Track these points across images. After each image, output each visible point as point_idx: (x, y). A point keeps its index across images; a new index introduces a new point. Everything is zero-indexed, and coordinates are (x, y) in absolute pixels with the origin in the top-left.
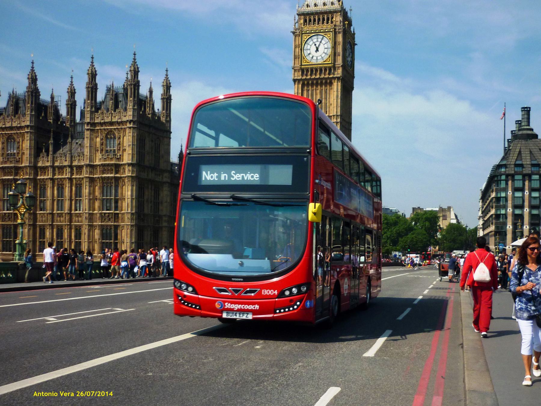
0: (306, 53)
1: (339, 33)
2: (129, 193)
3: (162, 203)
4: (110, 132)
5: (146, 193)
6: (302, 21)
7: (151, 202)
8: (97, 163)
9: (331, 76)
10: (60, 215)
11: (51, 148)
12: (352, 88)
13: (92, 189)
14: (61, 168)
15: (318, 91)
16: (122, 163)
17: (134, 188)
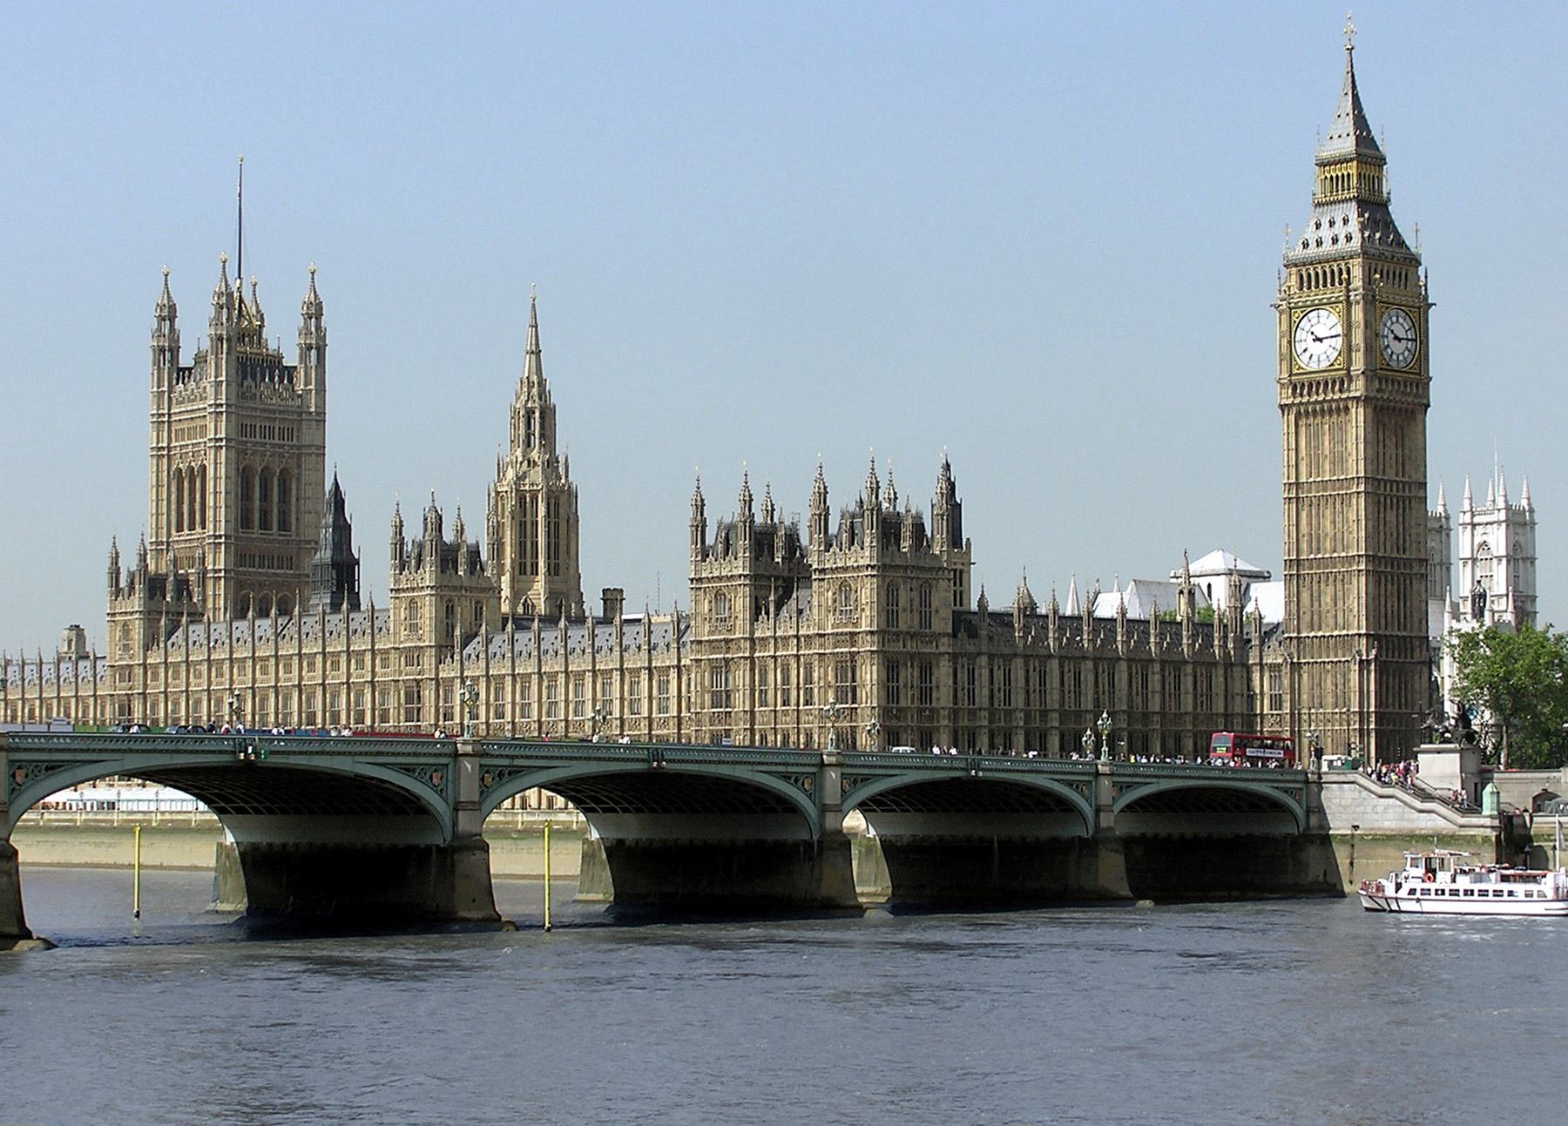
0: (1300, 347)
1: (1357, 302)
2: (868, 677)
3: (938, 687)
4: (844, 582)
5: (902, 674)
6: (1294, 280)
7: (912, 687)
8: (830, 631)
9: (1344, 396)
10: (785, 713)
11: (772, 610)
12: (1428, 406)
13: (822, 670)
14: (785, 639)
15: (1327, 426)
16: (858, 630)
17: (875, 668)
